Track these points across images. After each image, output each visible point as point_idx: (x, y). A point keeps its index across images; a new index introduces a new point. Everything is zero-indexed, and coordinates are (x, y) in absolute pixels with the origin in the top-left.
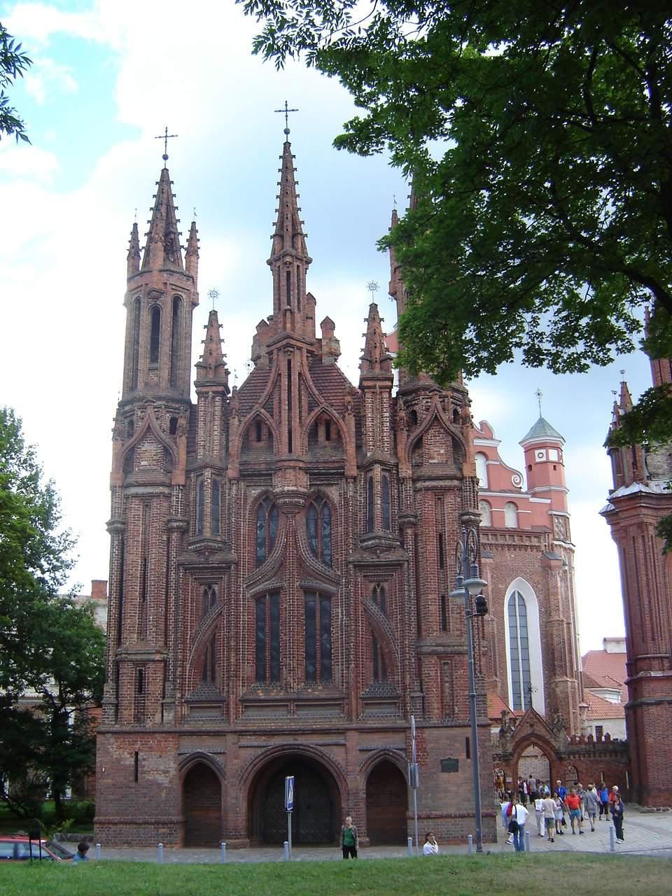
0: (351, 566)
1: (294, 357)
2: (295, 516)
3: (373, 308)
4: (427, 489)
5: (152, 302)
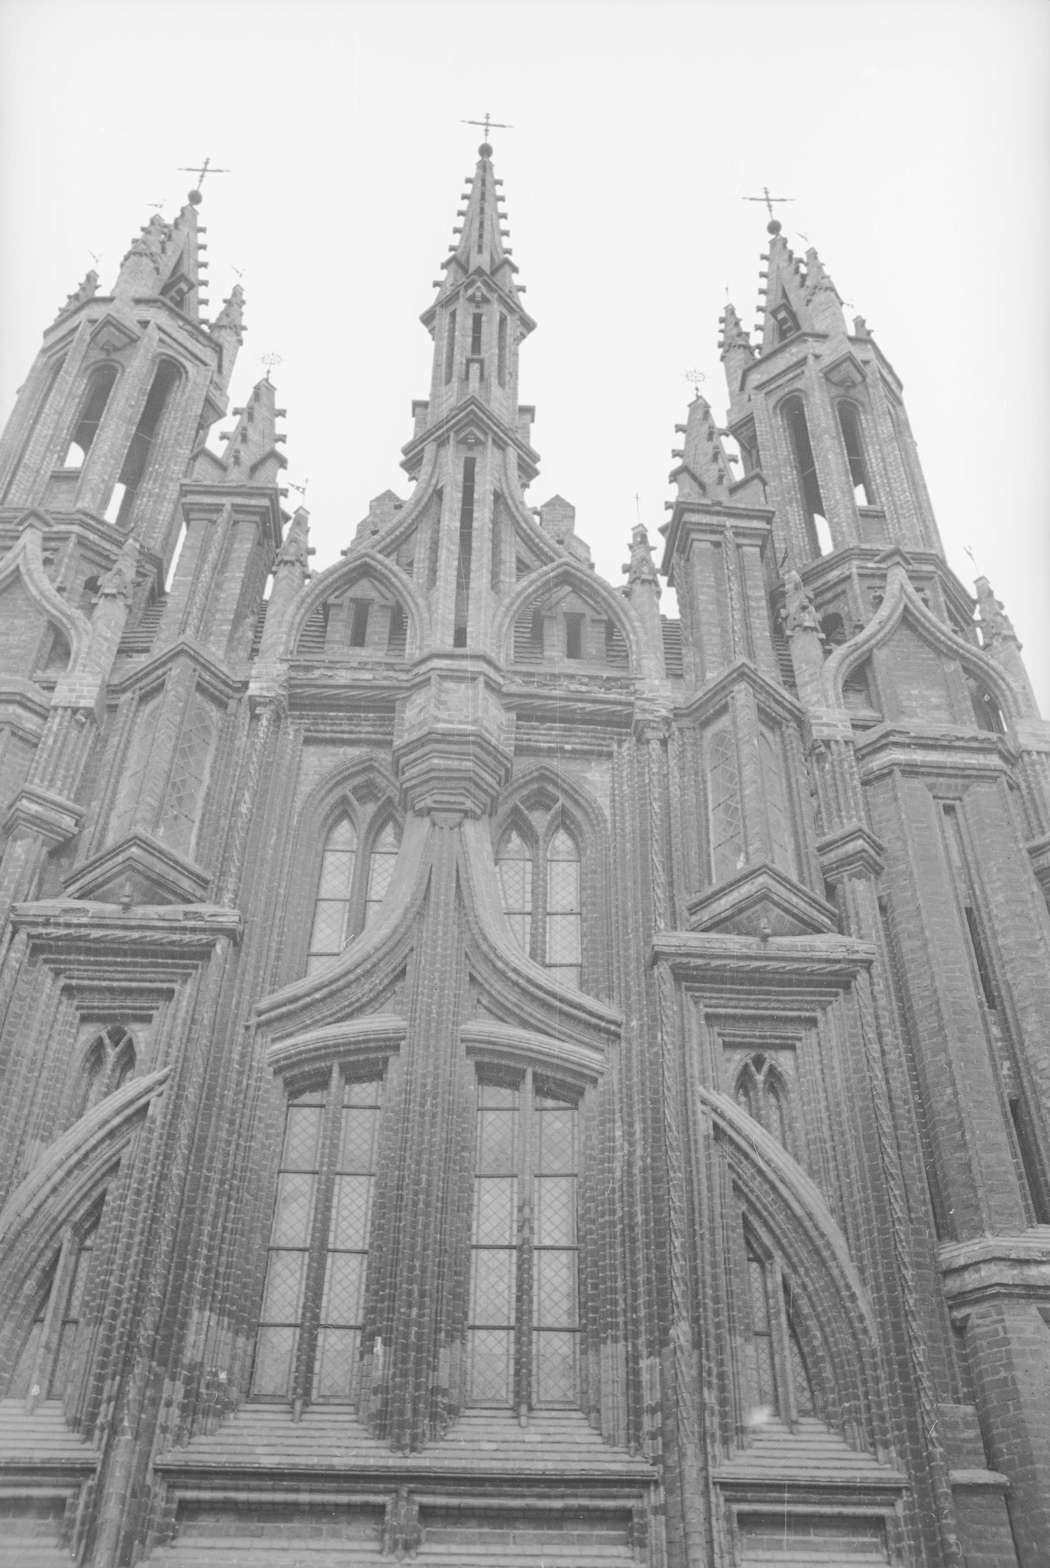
0: (663, 969)
1: (483, 454)
2: (460, 825)
3: (700, 409)
4: (911, 770)
5: (97, 355)
